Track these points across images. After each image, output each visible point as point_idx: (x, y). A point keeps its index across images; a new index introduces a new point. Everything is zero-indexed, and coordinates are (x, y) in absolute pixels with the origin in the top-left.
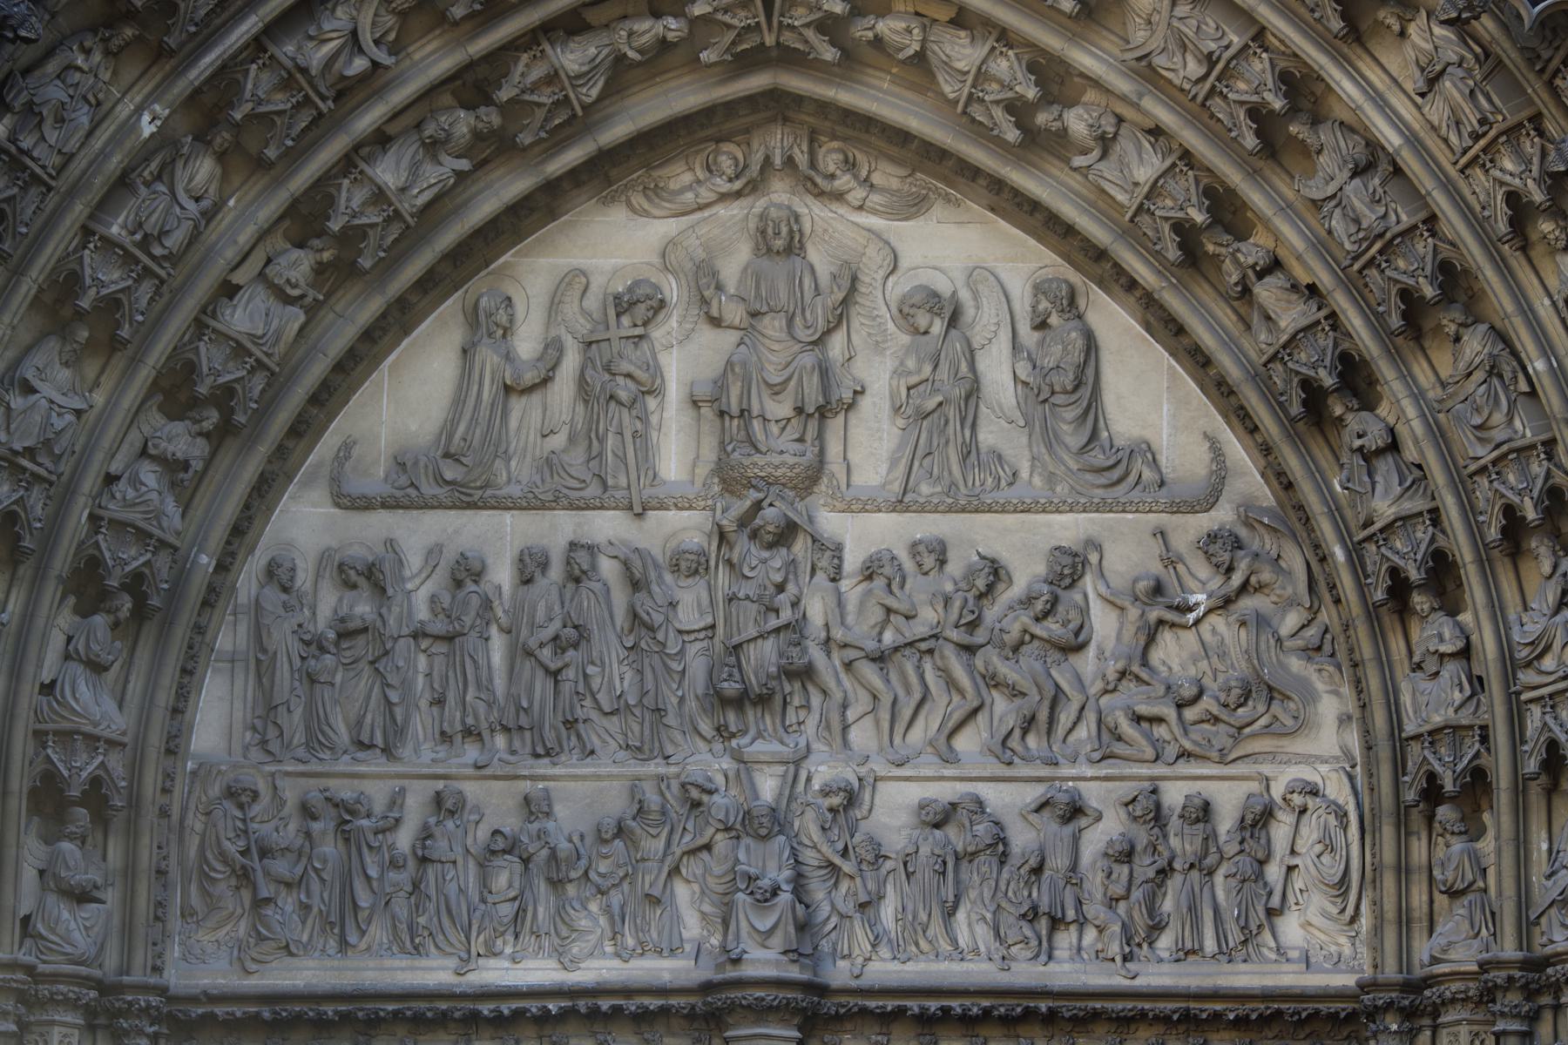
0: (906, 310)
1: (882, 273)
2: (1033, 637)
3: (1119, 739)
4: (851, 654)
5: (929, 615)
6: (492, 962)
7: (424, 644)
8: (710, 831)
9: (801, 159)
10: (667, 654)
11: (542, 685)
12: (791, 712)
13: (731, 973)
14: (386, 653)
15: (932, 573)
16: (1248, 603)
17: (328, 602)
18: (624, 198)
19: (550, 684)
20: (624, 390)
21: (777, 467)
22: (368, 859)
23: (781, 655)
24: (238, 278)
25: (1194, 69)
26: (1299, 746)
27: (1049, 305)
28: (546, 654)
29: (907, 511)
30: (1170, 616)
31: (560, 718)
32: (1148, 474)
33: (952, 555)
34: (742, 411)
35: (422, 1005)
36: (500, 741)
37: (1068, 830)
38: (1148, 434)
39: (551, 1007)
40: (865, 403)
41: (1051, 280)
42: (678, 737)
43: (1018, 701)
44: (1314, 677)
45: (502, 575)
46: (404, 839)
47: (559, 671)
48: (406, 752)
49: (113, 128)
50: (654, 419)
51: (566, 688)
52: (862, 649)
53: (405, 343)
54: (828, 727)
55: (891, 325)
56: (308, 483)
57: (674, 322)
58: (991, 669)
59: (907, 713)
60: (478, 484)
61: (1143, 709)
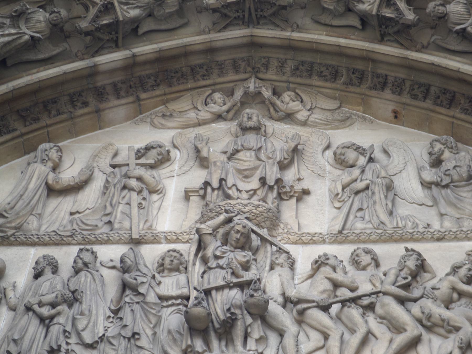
1: (321, 148)
2: (461, 294)
9: (267, 93)
10: (146, 303)
12: (251, 344)
15: (369, 268)
18: (149, 120)
19: (42, 331)
21: (246, 205)
27: (442, 147)
33: (381, 263)
34: (221, 180)
47: (52, 318)
50: (157, 205)
52: (313, 301)
55: (328, 168)
57: (176, 166)
58: (426, 311)
59: (355, 340)
60: (13, 225)
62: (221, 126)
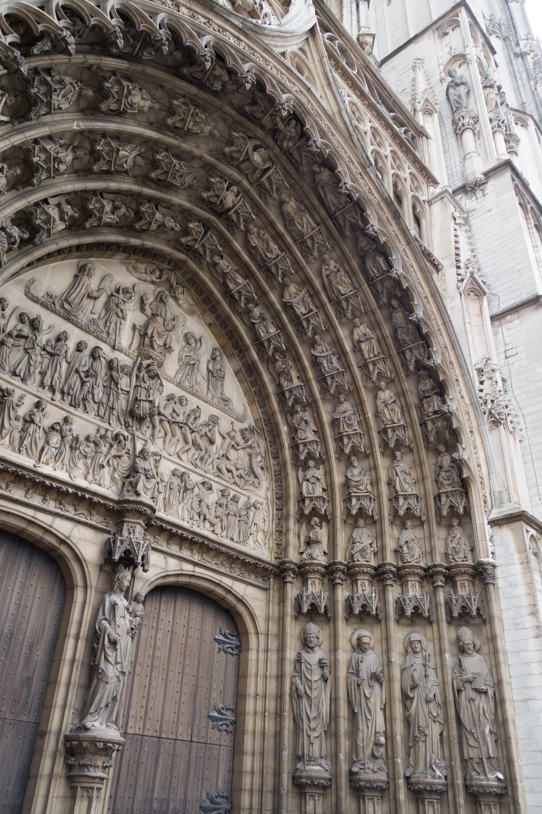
0: (189, 336)
1: (181, 324)
2: (206, 435)
3: (221, 473)
4: (164, 418)
5: (181, 419)
6: (46, 466)
7: (43, 353)
8: (124, 452)
11: (78, 383)
13: (134, 498)
14: (33, 348)
16: (249, 450)
17: (13, 324)
20: (120, 314)
22: (12, 412)
23: (150, 409)
24: (50, 200)
25: (303, 311)
26: (257, 491)
28: (82, 375)
29: (180, 387)
30: (235, 445)
31: (82, 397)
32: (232, 407)
35: (25, 473)
36: (58, 396)
37: (208, 492)
38: (231, 398)
39: (69, 489)
40: (173, 354)
41: (233, 345)
42: (115, 420)
43: (199, 451)
44: (262, 475)
45: (71, 344)
46: (22, 411)
47: (85, 382)
48: (29, 382)
49: (61, 118)
51: (86, 389)
53: (58, 263)
54: (153, 435)
56: (19, 283)
57: (132, 304)
61: (229, 467)
62: (152, 287)
